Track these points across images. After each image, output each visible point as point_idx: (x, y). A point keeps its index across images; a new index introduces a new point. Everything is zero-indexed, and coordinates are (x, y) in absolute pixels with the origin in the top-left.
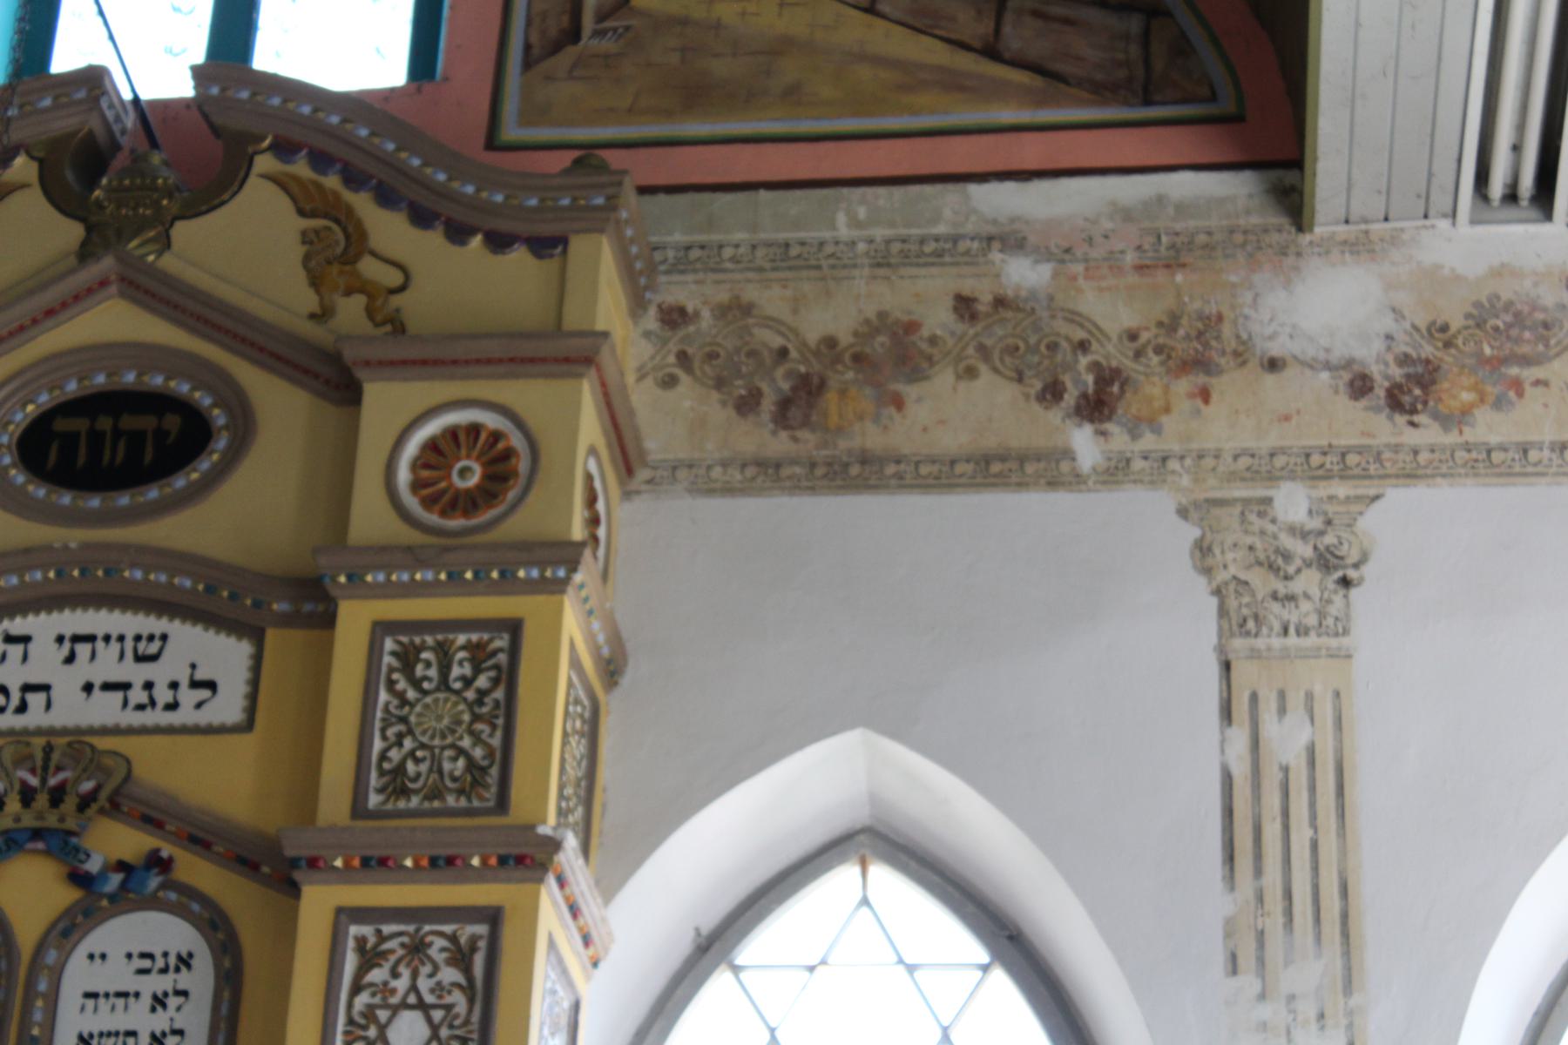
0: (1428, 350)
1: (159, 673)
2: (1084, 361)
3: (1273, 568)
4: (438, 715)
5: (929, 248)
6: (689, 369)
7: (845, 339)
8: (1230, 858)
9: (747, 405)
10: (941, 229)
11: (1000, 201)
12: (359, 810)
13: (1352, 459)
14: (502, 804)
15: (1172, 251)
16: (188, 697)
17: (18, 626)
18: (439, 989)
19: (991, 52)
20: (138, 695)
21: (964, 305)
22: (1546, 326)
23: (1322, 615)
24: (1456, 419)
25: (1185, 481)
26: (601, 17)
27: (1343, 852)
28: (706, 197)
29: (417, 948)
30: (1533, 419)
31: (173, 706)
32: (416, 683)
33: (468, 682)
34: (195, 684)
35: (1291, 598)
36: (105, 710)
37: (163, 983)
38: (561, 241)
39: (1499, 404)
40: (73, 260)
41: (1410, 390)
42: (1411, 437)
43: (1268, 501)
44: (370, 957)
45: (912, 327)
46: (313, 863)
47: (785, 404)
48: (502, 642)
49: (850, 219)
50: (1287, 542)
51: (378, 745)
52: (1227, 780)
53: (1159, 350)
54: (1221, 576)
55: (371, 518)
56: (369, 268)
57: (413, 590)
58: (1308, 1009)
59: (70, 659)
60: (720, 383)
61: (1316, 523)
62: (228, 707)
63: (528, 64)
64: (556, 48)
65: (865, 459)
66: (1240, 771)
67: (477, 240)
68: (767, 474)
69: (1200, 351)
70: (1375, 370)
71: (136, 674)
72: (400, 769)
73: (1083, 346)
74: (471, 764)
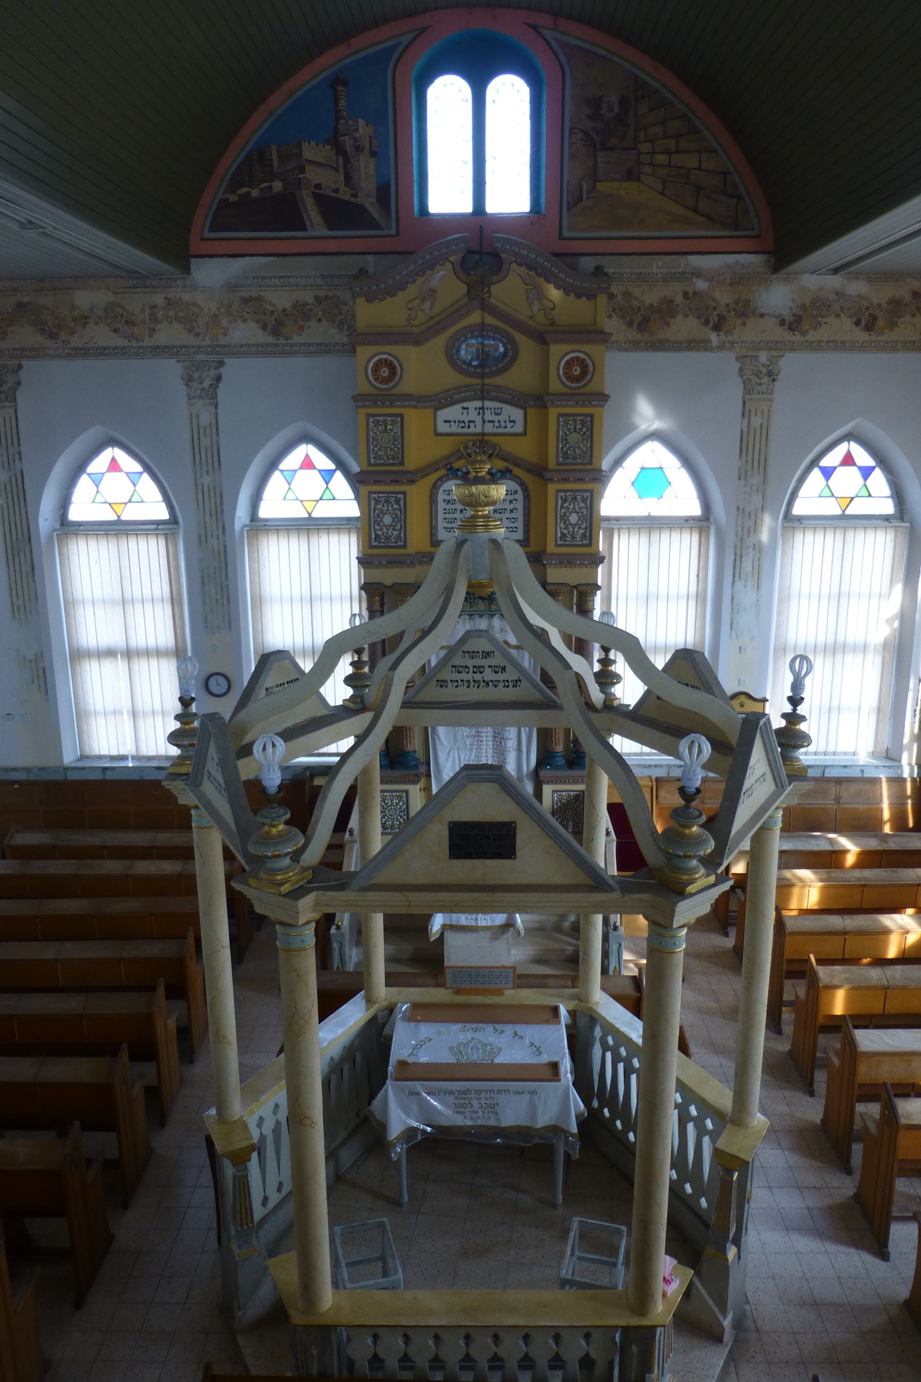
0: (800, 313)
1: (502, 418)
2: (715, 313)
3: (757, 376)
4: (574, 438)
5: (677, 276)
6: (615, 313)
7: (655, 305)
8: (741, 452)
9: (630, 324)
10: (680, 270)
11: (697, 261)
12: (558, 464)
13: (778, 344)
14: (591, 463)
15: (739, 279)
16: (509, 425)
17: (465, 405)
18: (580, 508)
19: (695, 211)
20: (497, 424)
21: (685, 294)
22: (829, 306)
23: (768, 389)
24: (804, 333)
25: (738, 350)
26: (588, 193)
27: (766, 452)
28: (619, 257)
29: (575, 499)
30: (822, 334)
31: (505, 427)
32: (569, 430)
33: (581, 430)
34: (510, 422)
35: (761, 384)
36: (489, 428)
37: (511, 497)
38: (594, 296)
39: (815, 329)
40: (466, 300)
41: (794, 324)
42: (793, 338)
43: (757, 356)
44: (565, 501)
45: (672, 301)
46: (550, 480)
47: (640, 324)
48: (589, 419)
49: (657, 266)
50: (761, 368)
51: (561, 446)
52: (742, 431)
53: (734, 310)
54: (745, 377)
55: (555, 385)
56: (544, 301)
57: (568, 406)
58: (755, 489)
59: (479, 414)
60: (623, 317)
61: (769, 363)
62: (519, 428)
63: (568, 209)
64: (576, 204)
65: (661, 341)
66: (745, 430)
67: (572, 295)
68: (636, 346)
69: (745, 310)
70: (787, 318)
71: (496, 418)
72: (566, 452)
73: (715, 308)
74: (583, 452)
